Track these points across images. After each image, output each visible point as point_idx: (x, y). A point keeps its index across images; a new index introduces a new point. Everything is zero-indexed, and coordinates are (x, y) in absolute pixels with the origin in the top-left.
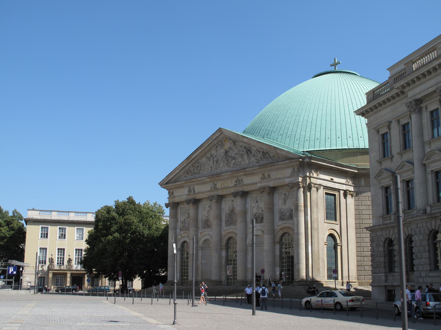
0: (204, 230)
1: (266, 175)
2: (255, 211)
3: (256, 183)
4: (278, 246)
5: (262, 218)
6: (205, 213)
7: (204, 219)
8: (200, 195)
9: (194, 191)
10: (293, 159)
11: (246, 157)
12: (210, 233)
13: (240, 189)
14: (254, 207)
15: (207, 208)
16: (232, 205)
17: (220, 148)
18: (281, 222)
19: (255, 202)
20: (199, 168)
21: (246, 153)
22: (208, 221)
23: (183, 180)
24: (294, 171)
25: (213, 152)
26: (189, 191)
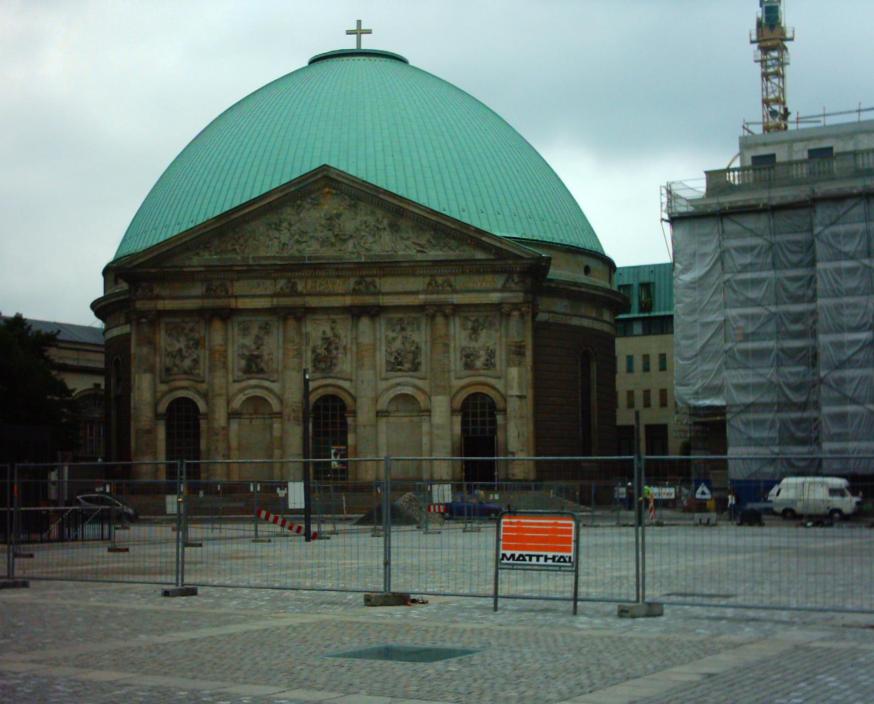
0: (246, 376)
1: (440, 280)
2: (397, 345)
3: (416, 293)
4: (458, 419)
5: (419, 363)
6: (249, 341)
7: (247, 353)
8: (247, 300)
9: (227, 292)
10: (521, 258)
11: (386, 237)
12: (266, 384)
13: (370, 300)
14: (394, 339)
15: (255, 331)
16: (332, 328)
17: (310, 206)
18: (468, 372)
19: (398, 327)
20: (241, 241)
21: (388, 229)
22: (257, 357)
23: (187, 263)
24: (513, 280)
25: (288, 213)
26: (208, 289)
